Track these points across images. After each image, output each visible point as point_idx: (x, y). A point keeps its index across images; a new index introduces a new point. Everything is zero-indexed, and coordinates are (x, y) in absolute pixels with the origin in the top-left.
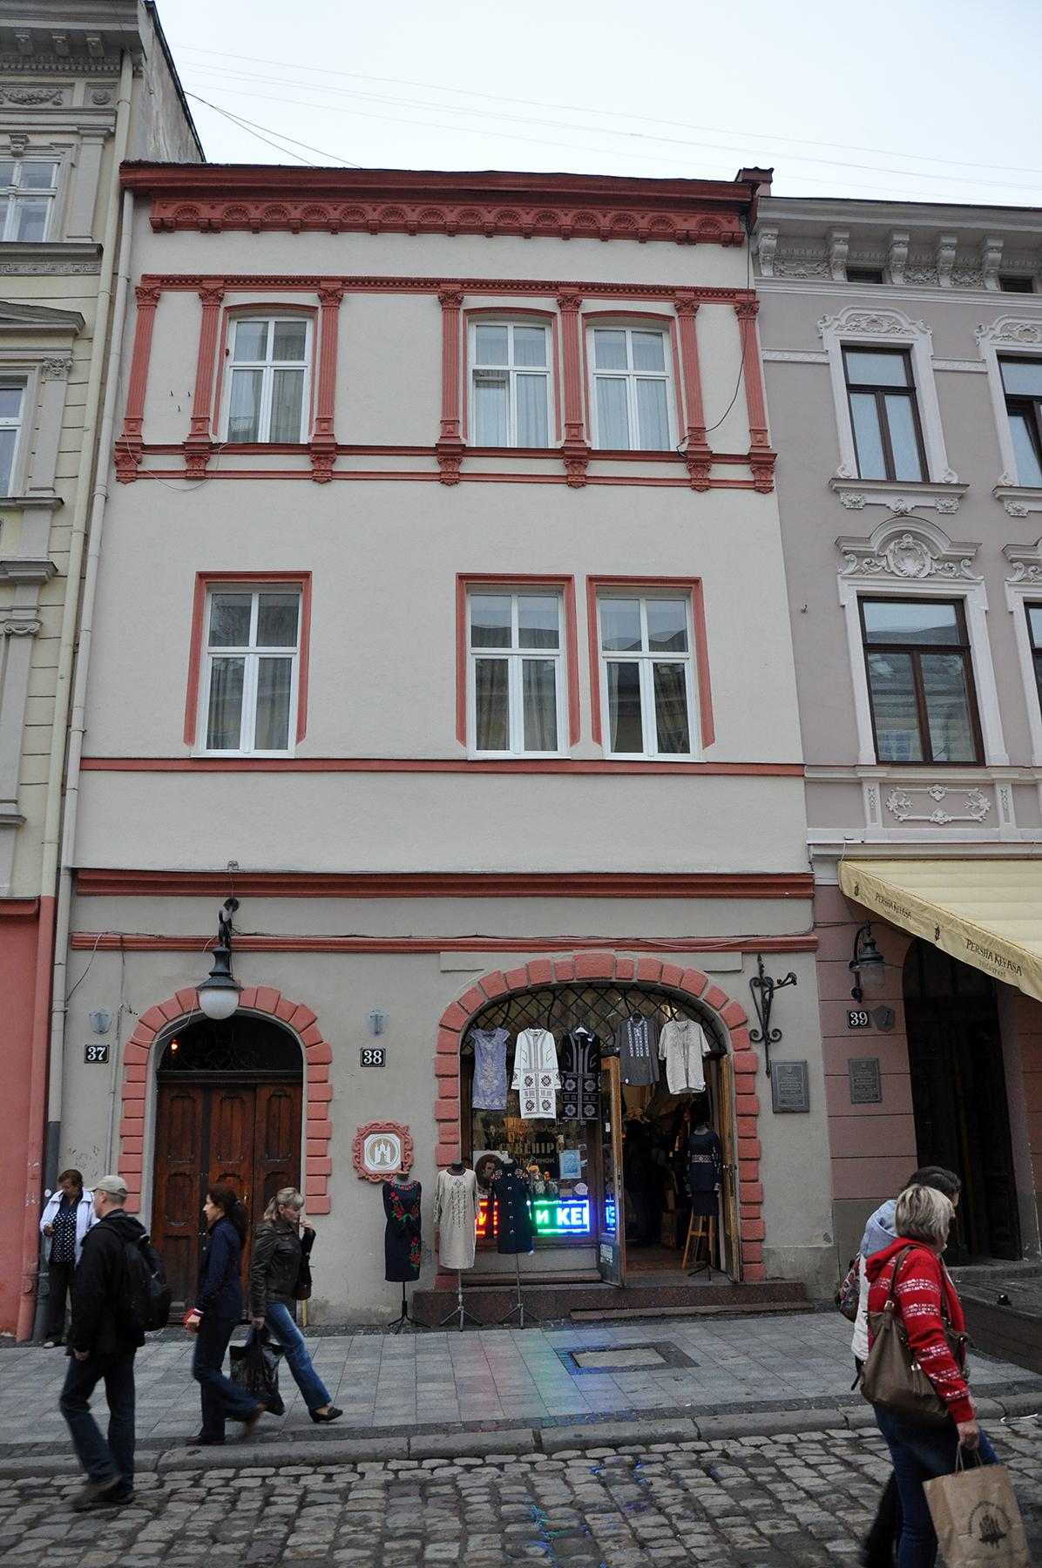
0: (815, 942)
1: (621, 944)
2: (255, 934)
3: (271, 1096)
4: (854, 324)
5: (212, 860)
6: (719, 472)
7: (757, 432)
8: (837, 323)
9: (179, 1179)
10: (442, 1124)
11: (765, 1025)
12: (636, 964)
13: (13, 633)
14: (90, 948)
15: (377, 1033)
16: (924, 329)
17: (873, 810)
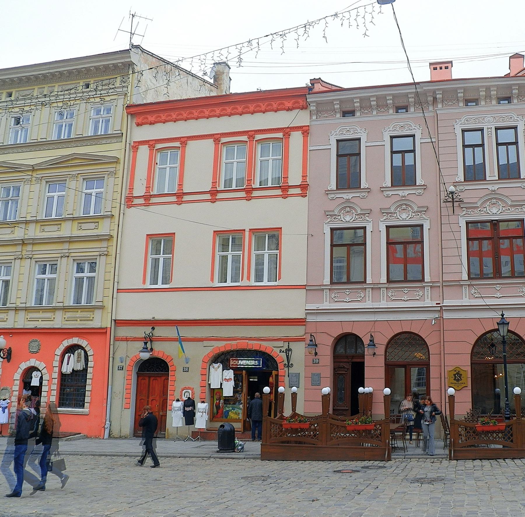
0: (304, 338)
1: (250, 339)
2: (158, 336)
3: (164, 379)
4: (341, 132)
5: (148, 316)
6: (291, 191)
7: (304, 176)
8: (336, 133)
9: (142, 400)
10: (202, 388)
11: (288, 363)
12: (254, 345)
13: (101, 255)
14: (119, 340)
15: (187, 363)
16: (365, 131)
17: (326, 298)
